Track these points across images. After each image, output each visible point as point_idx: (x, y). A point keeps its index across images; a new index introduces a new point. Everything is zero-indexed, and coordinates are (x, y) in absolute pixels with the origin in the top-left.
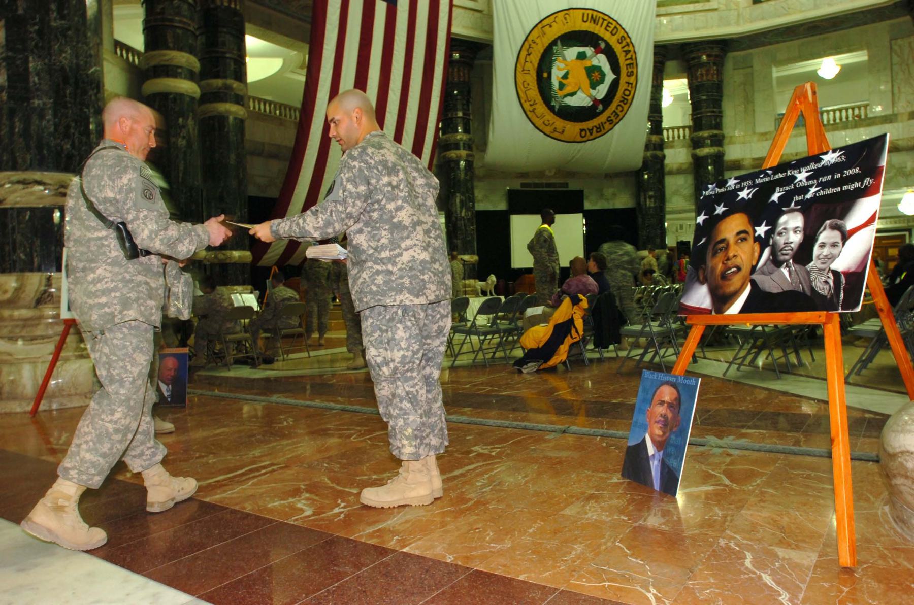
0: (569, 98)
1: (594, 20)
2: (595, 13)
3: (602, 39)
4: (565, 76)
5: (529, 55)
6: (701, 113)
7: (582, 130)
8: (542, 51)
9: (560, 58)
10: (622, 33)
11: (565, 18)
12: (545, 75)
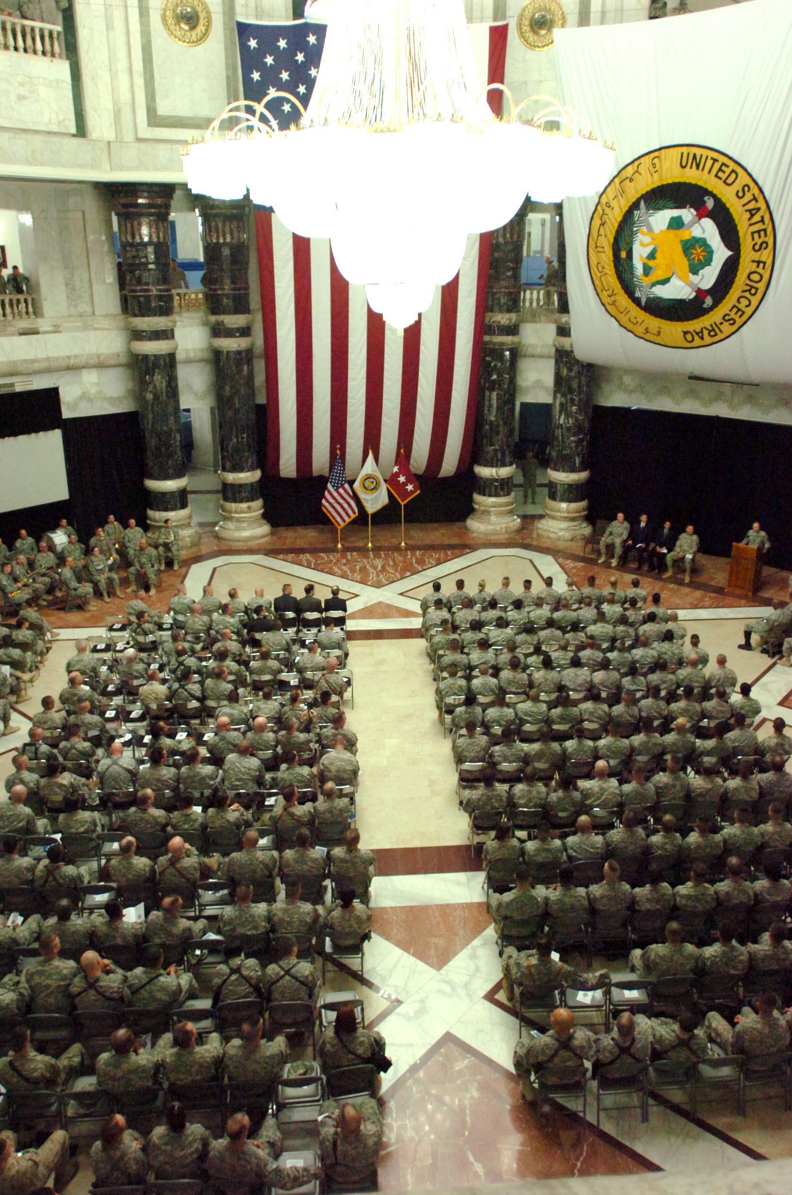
0: (659, 287)
1: (696, 162)
2: (698, 152)
4: (652, 256)
7: (685, 333)
8: (620, 219)
9: (644, 229)
10: (743, 179)
11: (654, 165)
12: (623, 255)
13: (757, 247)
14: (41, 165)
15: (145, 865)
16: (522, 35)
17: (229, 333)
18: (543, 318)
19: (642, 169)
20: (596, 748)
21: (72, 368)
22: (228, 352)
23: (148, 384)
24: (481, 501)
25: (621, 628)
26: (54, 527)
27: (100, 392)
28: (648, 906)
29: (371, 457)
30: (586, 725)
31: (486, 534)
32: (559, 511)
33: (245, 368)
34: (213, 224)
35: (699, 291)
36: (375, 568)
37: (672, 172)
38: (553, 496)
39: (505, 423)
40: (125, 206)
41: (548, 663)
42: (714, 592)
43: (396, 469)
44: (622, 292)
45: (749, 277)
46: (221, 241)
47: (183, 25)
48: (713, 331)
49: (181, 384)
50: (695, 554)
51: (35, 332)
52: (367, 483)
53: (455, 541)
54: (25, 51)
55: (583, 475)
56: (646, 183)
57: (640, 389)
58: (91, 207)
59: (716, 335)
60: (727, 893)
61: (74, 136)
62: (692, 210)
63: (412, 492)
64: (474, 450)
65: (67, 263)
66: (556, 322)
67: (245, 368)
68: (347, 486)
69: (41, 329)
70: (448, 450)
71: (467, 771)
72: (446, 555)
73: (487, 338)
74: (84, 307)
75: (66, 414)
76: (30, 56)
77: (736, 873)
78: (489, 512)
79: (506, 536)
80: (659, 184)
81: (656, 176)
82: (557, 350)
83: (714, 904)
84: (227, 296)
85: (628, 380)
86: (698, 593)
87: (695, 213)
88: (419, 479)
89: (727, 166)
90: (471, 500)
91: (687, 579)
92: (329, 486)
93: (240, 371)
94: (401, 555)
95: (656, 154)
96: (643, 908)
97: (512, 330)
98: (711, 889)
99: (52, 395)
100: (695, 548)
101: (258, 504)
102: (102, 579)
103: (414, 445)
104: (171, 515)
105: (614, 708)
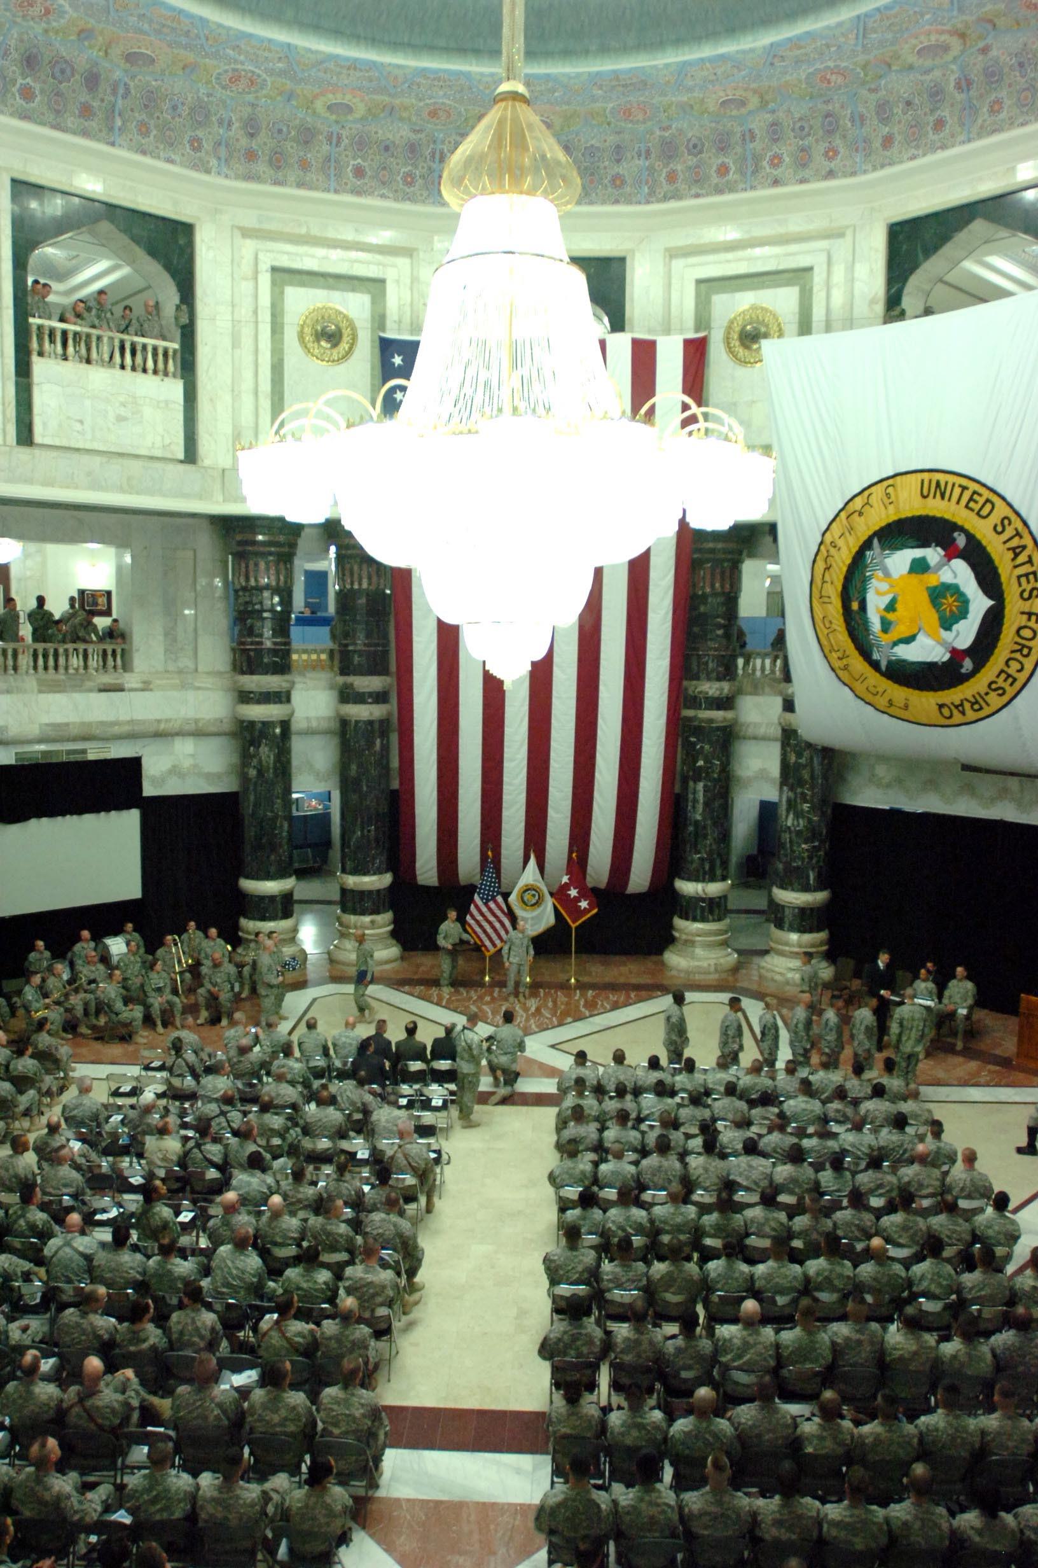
0: (902, 646)
1: (941, 491)
2: (942, 478)
3: (962, 529)
4: (891, 607)
5: (828, 568)
7: (941, 706)
8: (849, 561)
9: (880, 574)
10: (1001, 510)
11: (888, 495)
12: (855, 606)
13: (1026, 595)
14: (138, 493)
15: (51, 1398)
16: (730, 350)
17: (359, 698)
18: (767, 689)
19: (873, 500)
20: (752, 1276)
21: (162, 734)
22: (357, 722)
23: (252, 757)
24: (684, 927)
25: (836, 1105)
26: (116, 932)
27: (195, 766)
28: (774, 1532)
29: (532, 861)
30: (753, 1241)
31: (688, 972)
32: (787, 944)
33: (378, 741)
34: (348, 566)
35: (954, 652)
36: (526, 1010)
37: (909, 503)
38: (780, 925)
39: (715, 824)
40: (240, 543)
41: (711, 1146)
42: (998, 1064)
43: (565, 879)
44: (856, 653)
45: (1018, 632)
46: (356, 586)
47: (323, 343)
48: (977, 703)
49: (295, 762)
50: (971, 1009)
51: (120, 689)
52: (527, 897)
53: (645, 980)
54: (134, 369)
55: (820, 897)
56: (879, 517)
57: (899, 781)
58: (205, 544)
59: (981, 708)
60: (905, 1523)
61: (181, 462)
63: (586, 911)
64: (673, 857)
65: (171, 609)
66: (781, 693)
67: (378, 741)
68: (500, 899)
69: (127, 686)
70: (636, 856)
71: (562, 1297)
72: (628, 997)
73: (688, 713)
74: (186, 662)
75: (149, 790)
76: (140, 377)
77: (923, 1491)
78: (692, 943)
79: (716, 976)
80: (894, 518)
81: (891, 508)
82: (784, 730)
83: (884, 1540)
84: (360, 653)
85: (881, 771)
86: (973, 1065)
87: (942, 553)
88: (595, 894)
89: (980, 495)
90: (671, 927)
91: (960, 1045)
92: (476, 897)
93: (370, 744)
94: (568, 996)
95: (890, 482)
96: (767, 1537)
97: (726, 703)
98: (879, 1513)
99: (132, 767)
100: (970, 1001)
101: (387, 917)
102: (157, 1002)
103: (592, 849)
104: (270, 925)
105: (797, 1219)
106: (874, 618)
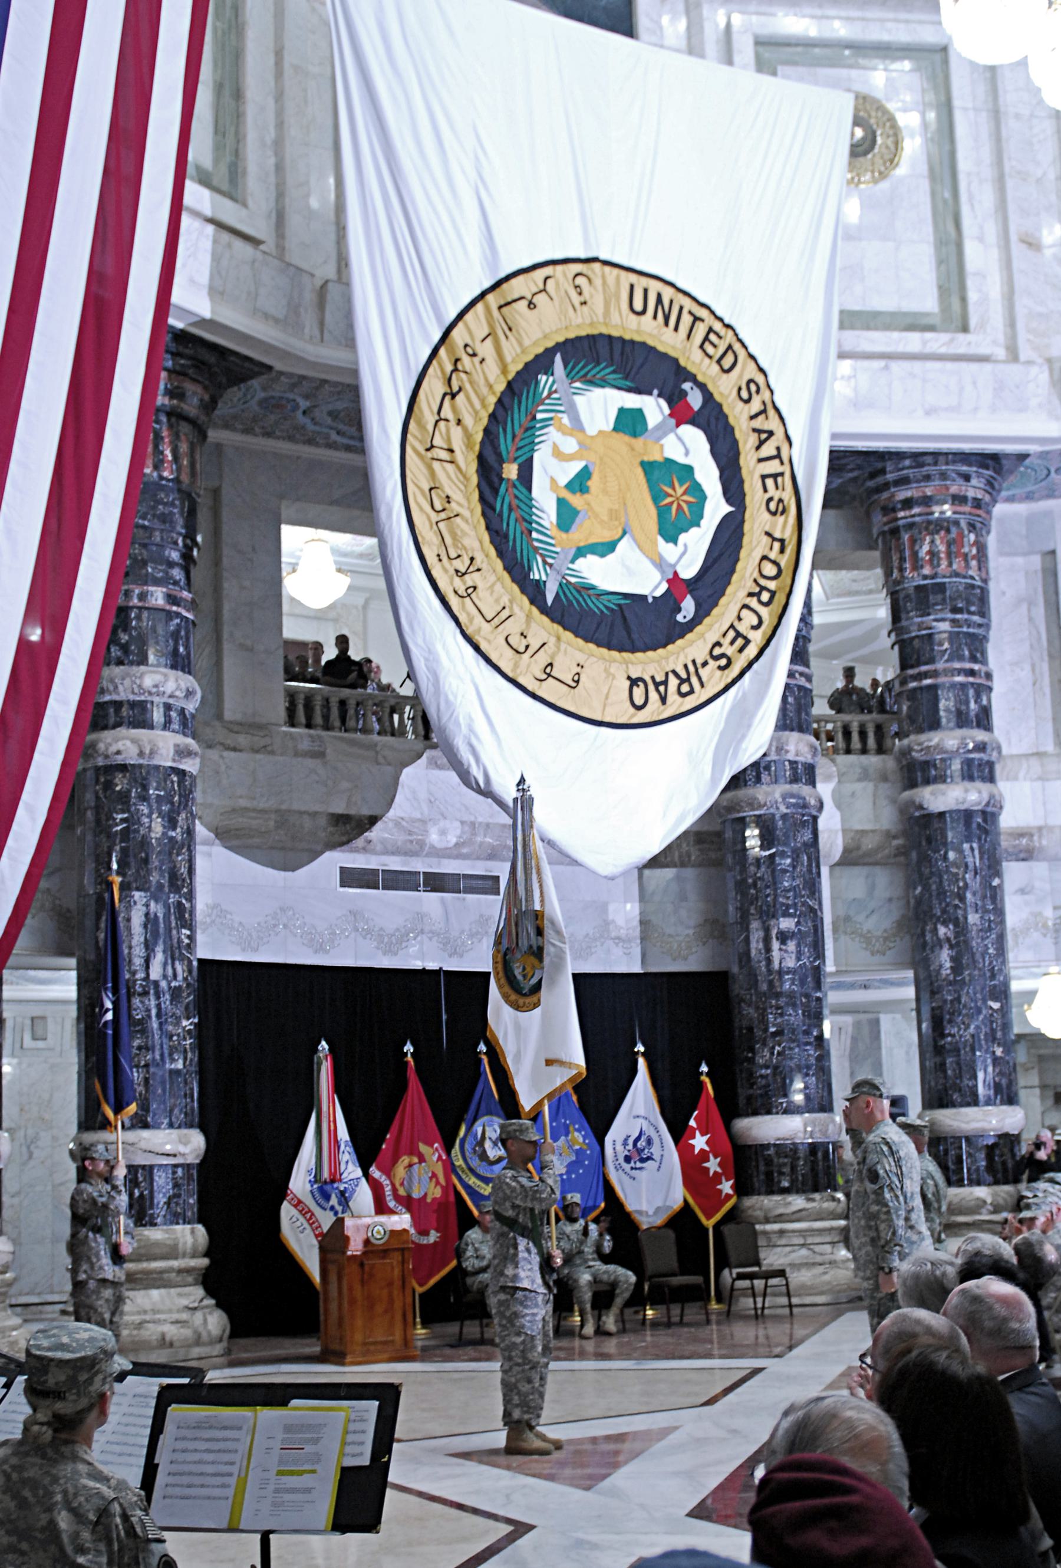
3: (693, 378)
4: (580, 483)
6: (935, 674)
9: (565, 420)
59: (692, 691)
62: (663, 403)
87: (667, 410)
106: (544, 497)
